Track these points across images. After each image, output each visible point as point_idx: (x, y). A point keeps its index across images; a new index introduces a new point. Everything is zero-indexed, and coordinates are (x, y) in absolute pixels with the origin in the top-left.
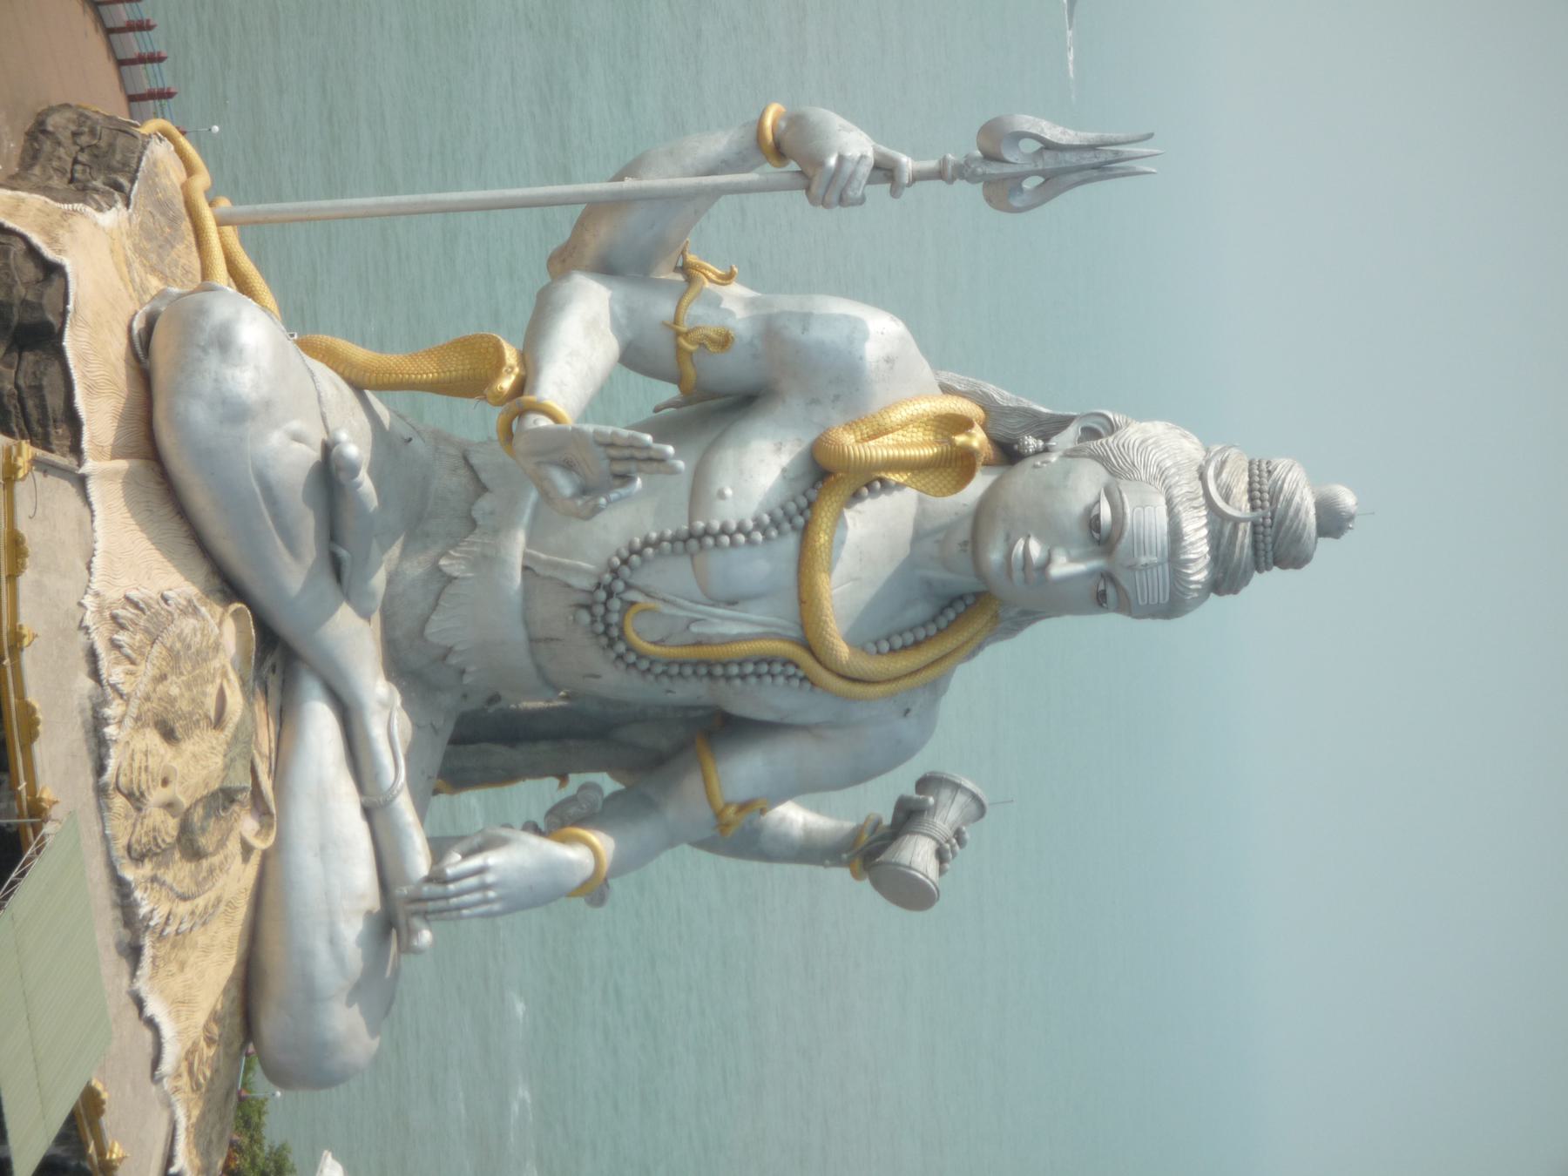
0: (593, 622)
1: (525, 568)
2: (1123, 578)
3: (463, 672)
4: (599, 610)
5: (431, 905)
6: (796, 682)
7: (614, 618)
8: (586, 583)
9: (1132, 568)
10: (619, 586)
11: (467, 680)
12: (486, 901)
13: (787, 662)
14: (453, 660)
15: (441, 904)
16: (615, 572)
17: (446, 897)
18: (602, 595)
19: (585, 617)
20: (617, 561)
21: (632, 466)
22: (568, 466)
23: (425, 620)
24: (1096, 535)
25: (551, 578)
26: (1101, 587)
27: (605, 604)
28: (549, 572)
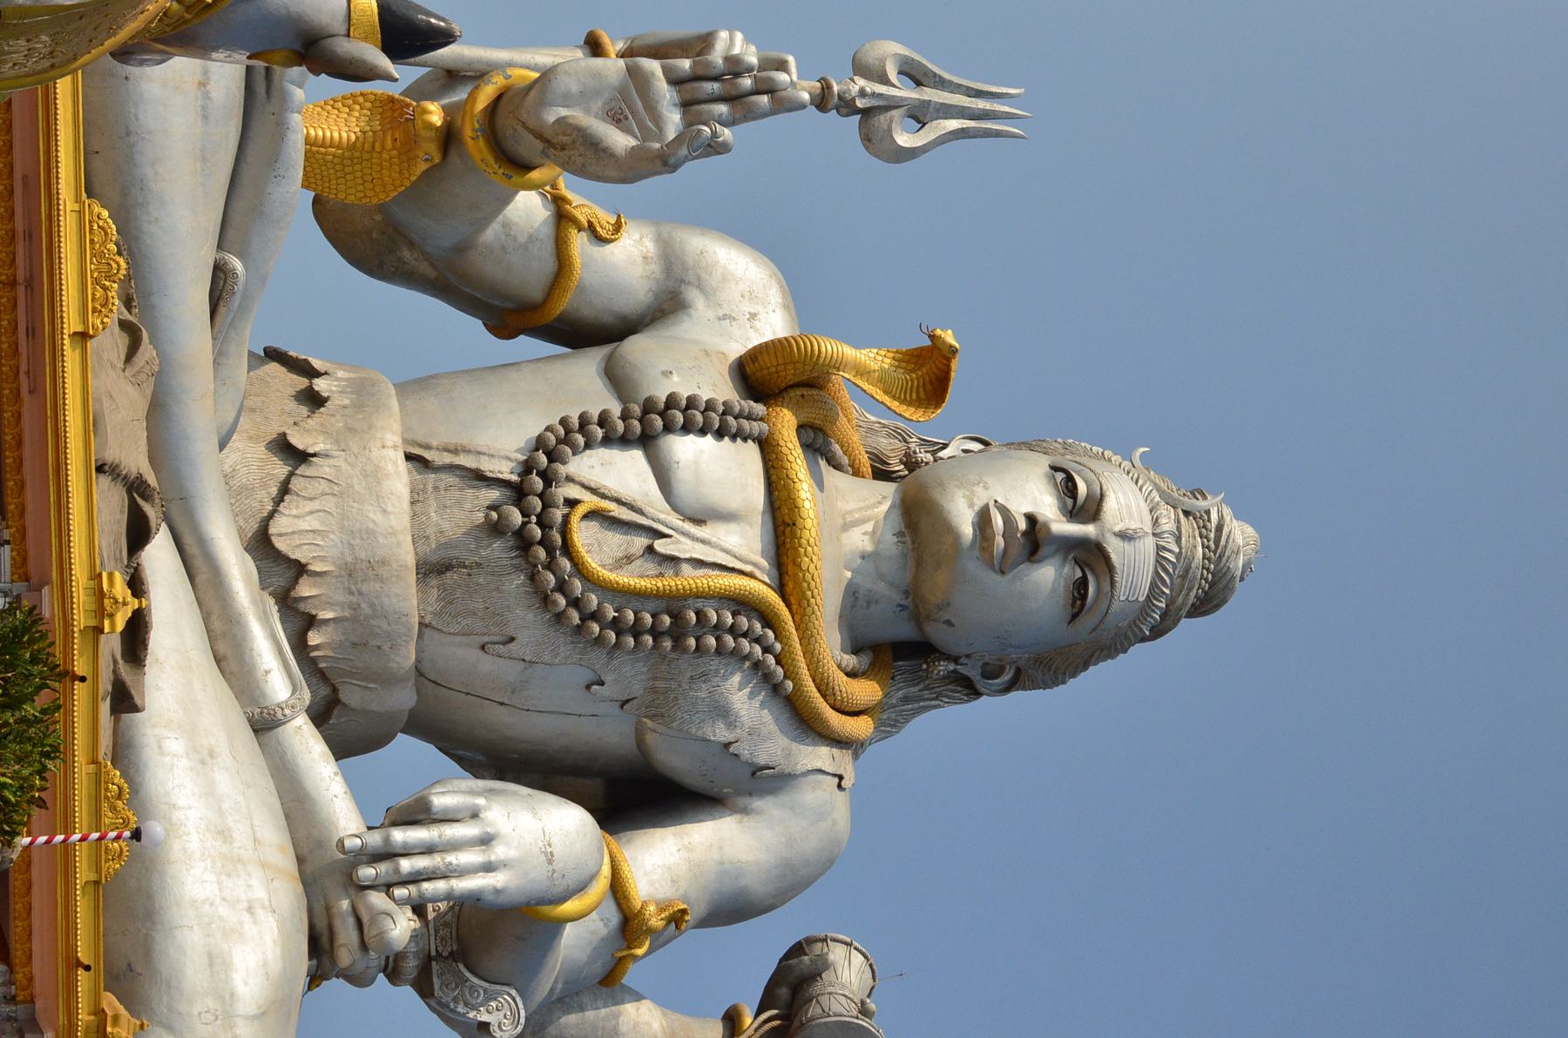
0: (524, 524)
1: (409, 457)
2: (1114, 548)
3: (311, 622)
4: (537, 504)
5: (406, 865)
6: (771, 660)
7: (558, 514)
8: (505, 470)
9: (1124, 536)
10: (562, 470)
11: (314, 638)
12: (488, 868)
13: (769, 620)
14: (305, 589)
15: (422, 863)
16: (552, 456)
17: (429, 850)
18: (538, 483)
19: (516, 517)
20: (552, 439)
21: (723, 108)
22: (618, 120)
23: (271, 515)
24: (1070, 501)
25: (452, 468)
26: (1079, 574)
27: (541, 496)
28: (448, 459)
